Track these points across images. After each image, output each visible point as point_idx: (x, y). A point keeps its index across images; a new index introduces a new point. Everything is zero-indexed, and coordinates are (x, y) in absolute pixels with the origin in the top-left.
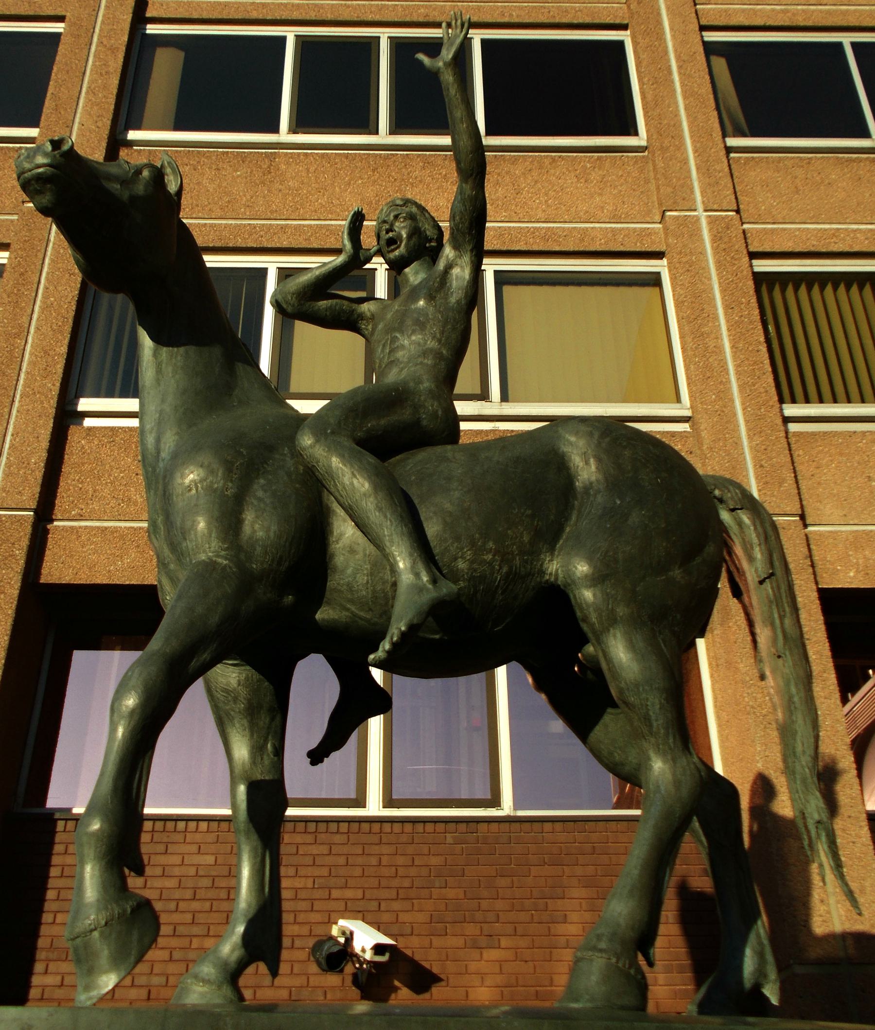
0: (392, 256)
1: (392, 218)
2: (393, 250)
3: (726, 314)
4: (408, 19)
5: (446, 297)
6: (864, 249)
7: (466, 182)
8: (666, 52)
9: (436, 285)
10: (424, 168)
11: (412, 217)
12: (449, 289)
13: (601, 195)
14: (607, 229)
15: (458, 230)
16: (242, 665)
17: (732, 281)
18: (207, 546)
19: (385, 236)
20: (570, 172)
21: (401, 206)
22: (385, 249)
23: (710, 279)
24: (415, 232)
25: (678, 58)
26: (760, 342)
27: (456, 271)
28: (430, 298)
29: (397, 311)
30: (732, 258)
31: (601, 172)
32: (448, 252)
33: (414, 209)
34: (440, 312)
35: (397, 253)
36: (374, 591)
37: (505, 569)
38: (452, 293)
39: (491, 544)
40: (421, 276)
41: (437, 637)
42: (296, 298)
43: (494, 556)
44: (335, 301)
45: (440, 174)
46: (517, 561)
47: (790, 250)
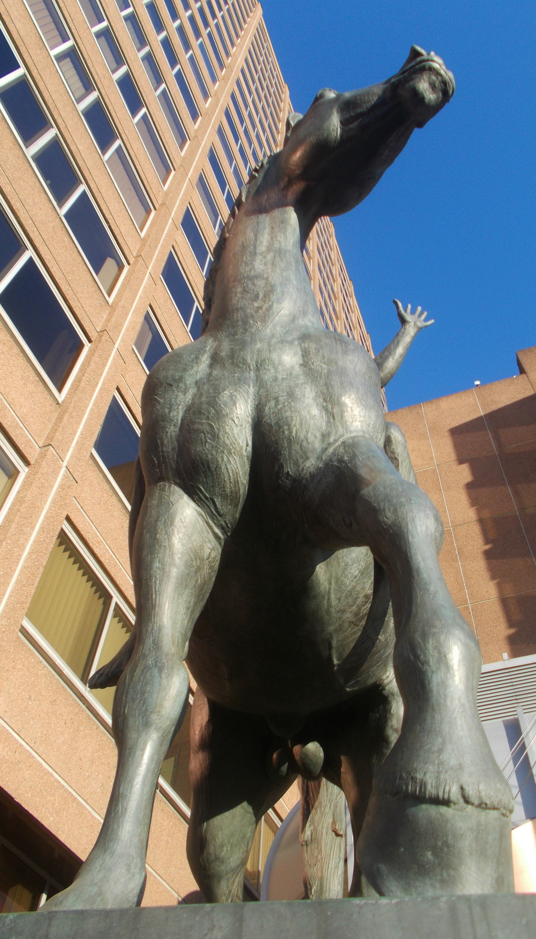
3: (39, 532)
8: (101, 375)
13: (25, 399)
14: (15, 419)
16: (220, 544)
17: (54, 517)
20: (21, 369)
23: (45, 504)
25: (103, 384)
26: (42, 565)
30: (62, 505)
31: (34, 389)
36: (354, 587)
41: (336, 662)
47: (79, 529)
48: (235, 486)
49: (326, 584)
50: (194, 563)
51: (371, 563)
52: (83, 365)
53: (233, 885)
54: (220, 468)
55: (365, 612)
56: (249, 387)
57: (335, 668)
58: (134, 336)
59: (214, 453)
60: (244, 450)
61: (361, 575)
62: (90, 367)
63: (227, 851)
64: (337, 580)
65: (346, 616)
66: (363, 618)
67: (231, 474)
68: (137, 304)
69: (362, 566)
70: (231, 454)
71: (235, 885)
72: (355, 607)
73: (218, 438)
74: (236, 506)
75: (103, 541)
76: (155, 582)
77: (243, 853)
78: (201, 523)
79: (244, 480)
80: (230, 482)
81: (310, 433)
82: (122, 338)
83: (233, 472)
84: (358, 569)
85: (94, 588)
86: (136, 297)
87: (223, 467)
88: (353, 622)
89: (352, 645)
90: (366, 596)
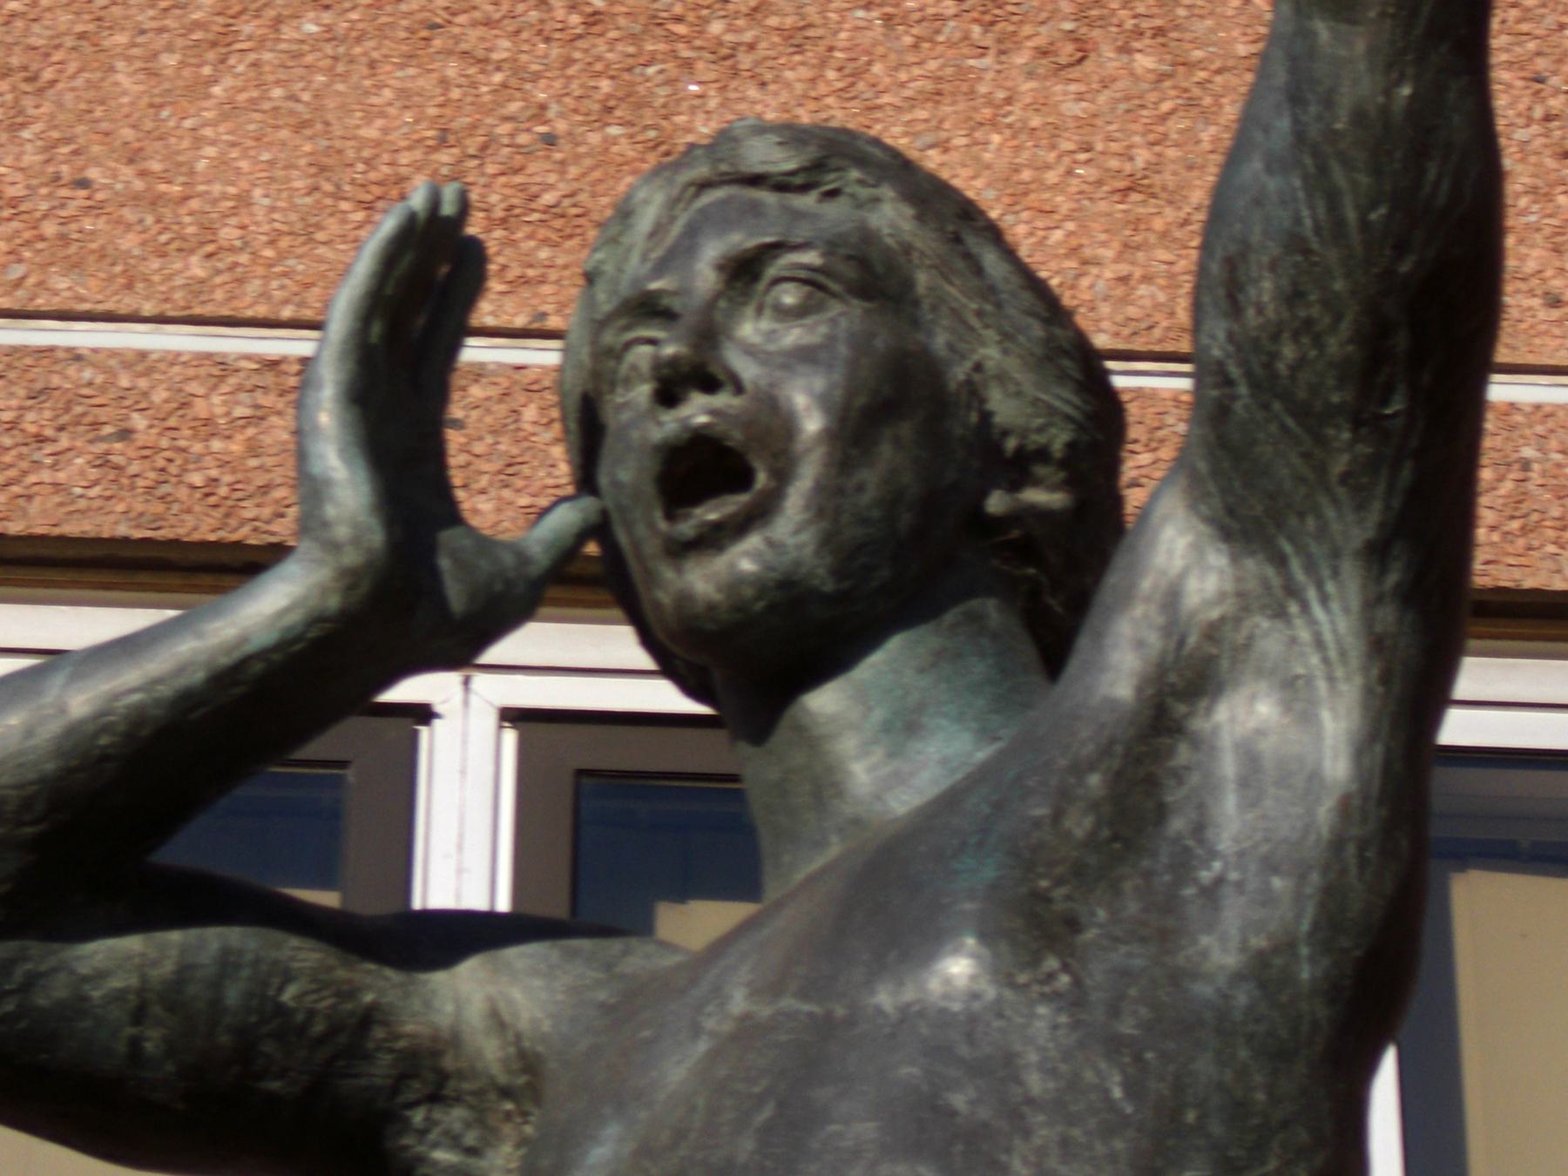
0: (703, 580)
1: (705, 275)
2: (713, 539)
5: (1164, 927)
9: (1079, 824)
11: (870, 276)
12: (1183, 865)
15: (1266, 385)
19: (644, 424)
21: (782, 185)
22: (645, 529)
24: (899, 396)
27: (1245, 715)
28: (1035, 928)
29: (747, 1032)
32: (1178, 557)
33: (891, 217)
34: (1114, 1046)
35: (745, 558)
38: (1211, 893)
40: (946, 753)
44: (210, 941)
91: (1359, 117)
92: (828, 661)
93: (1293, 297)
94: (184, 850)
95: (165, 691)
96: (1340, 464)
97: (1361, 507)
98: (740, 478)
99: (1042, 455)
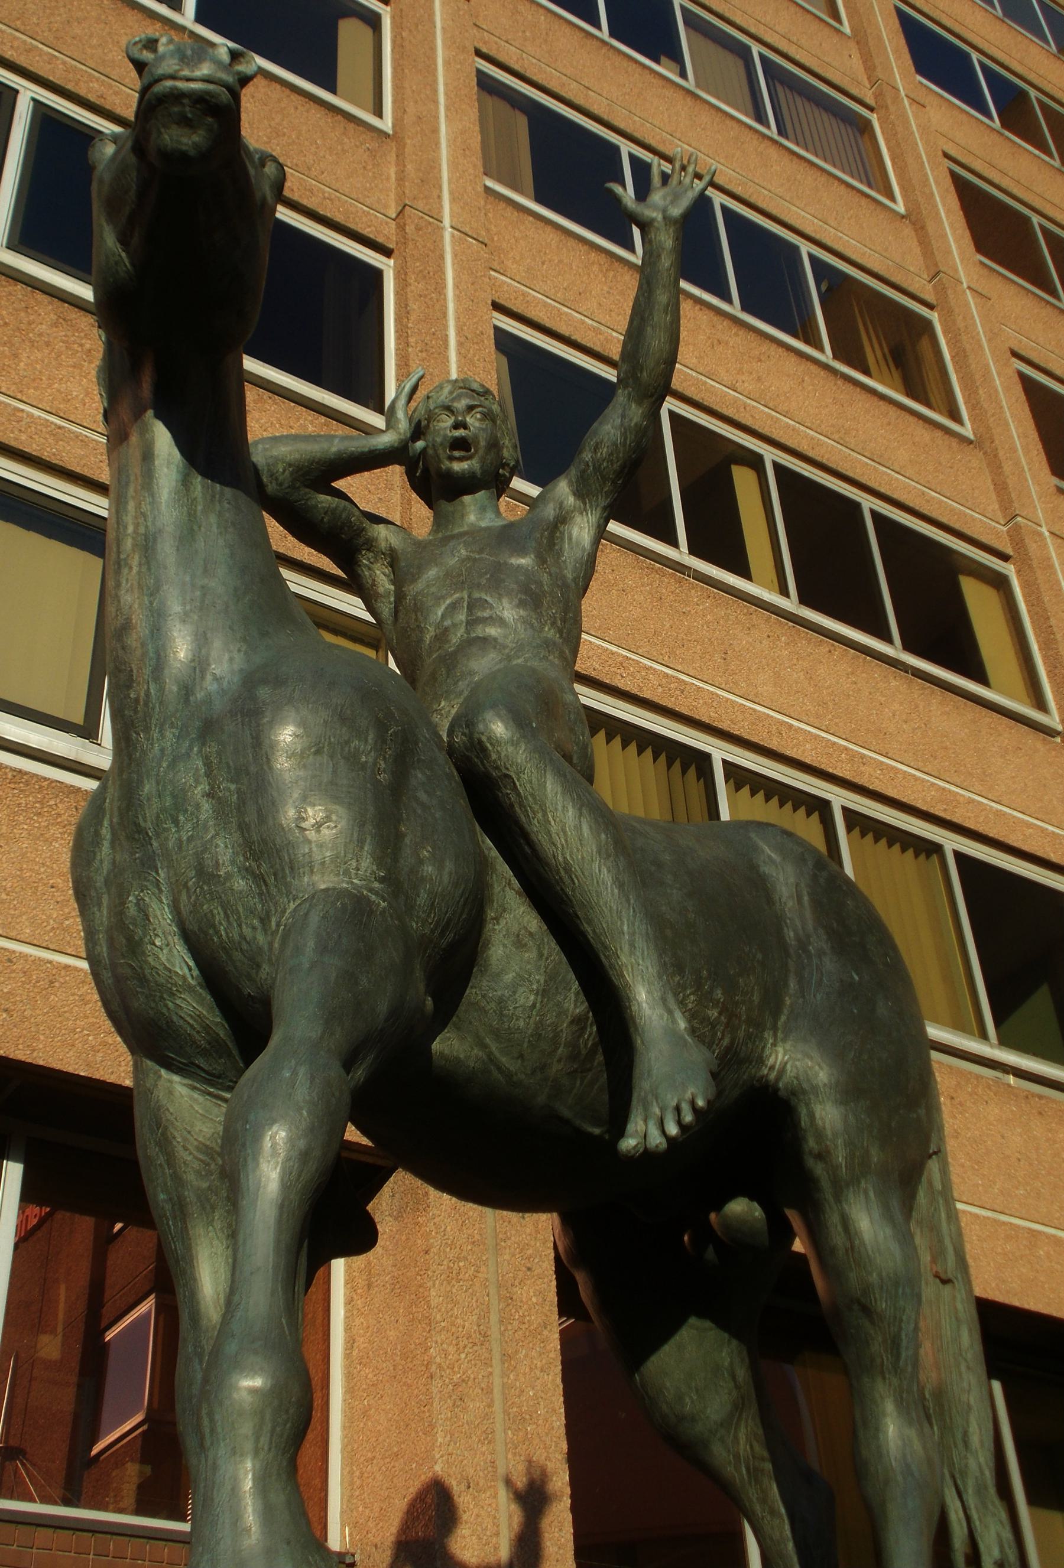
2: (461, 459)
4: (70, 87)
6: (656, 700)
7: (639, 403)
8: (445, 315)
10: (55, 325)
18: (354, 864)
25: (459, 331)
36: (540, 1024)
37: (726, 1042)
39: (719, 994)
41: (597, 1131)
42: (292, 473)
43: (720, 1014)
45: (81, 345)
46: (741, 1034)
48: (208, 1033)
49: (476, 1052)
50: (213, 1166)
51: (561, 962)
52: (398, 320)
53: (738, 1443)
54: (172, 1021)
55: (590, 1043)
56: (157, 872)
57: (607, 1137)
58: (475, 166)
59: (153, 1005)
60: (190, 979)
61: (543, 997)
62: (413, 317)
63: (692, 1402)
64: (496, 1034)
65: (554, 1070)
66: (592, 1052)
67: (191, 1022)
68: (446, 85)
69: (538, 982)
70: (174, 995)
71: (742, 1441)
72: (561, 1049)
73: (147, 981)
74: (230, 1055)
75: (629, 655)
76: (168, 1224)
77: (730, 1394)
78: (201, 1099)
79: (214, 1018)
80: (198, 1032)
81: (244, 927)
82: (451, 193)
83: (192, 1017)
84: (532, 991)
85: (663, 758)
86: (436, 69)
87: (175, 1019)
88: (575, 1071)
89: (606, 1097)
90: (579, 1021)
91: (636, 424)
92: (471, 490)
93: (611, 454)
94: (340, 484)
95: (359, 450)
96: (606, 489)
97: (606, 498)
98: (468, 450)
99: (508, 465)
